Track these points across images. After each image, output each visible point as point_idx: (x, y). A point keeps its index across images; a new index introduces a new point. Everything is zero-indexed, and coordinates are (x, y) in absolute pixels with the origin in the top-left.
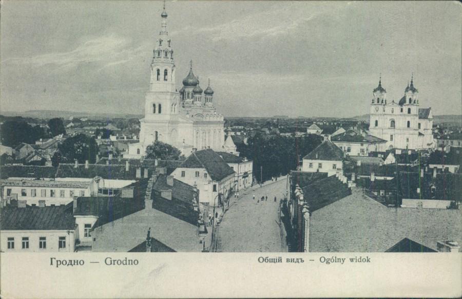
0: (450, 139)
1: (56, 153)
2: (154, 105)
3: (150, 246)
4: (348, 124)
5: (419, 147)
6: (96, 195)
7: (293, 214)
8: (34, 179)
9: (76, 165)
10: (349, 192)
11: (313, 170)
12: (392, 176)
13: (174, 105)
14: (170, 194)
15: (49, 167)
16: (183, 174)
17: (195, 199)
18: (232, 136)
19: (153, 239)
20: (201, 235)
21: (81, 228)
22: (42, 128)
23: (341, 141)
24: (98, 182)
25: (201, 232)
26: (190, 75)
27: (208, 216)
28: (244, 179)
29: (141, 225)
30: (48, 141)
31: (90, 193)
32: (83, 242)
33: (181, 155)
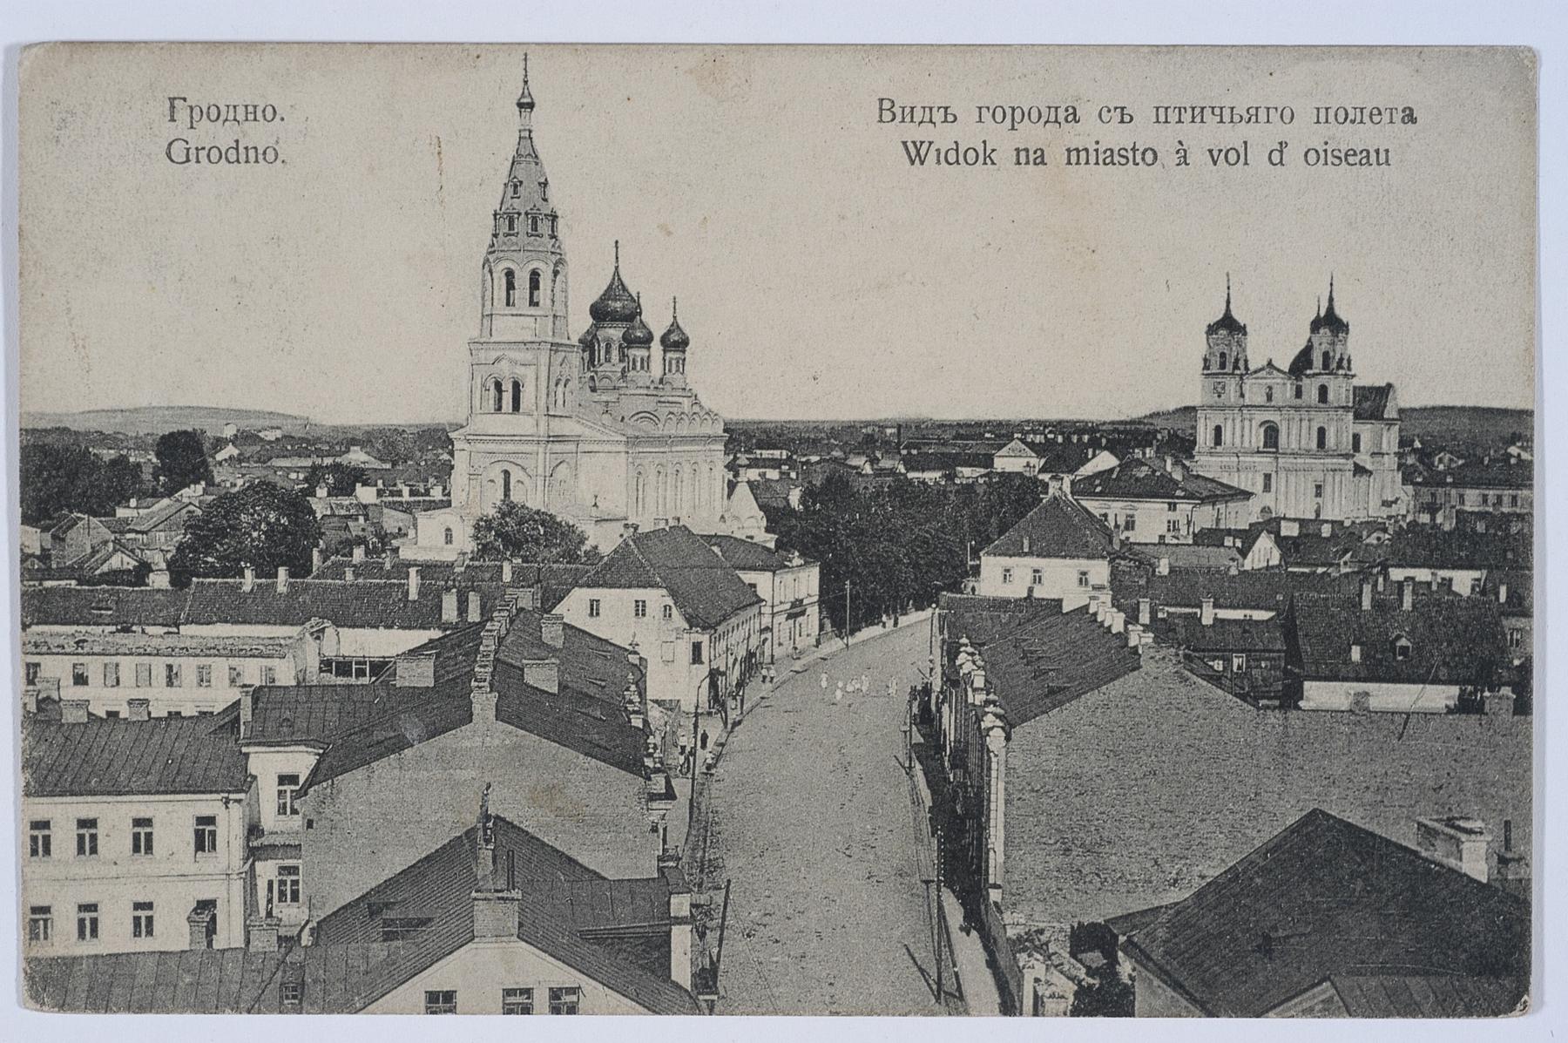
0: (1454, 485)
1: (181, 544)
2: (498, 386)
3: (487, 841)
4: (1125, 437)
6: (314, 678)
8: (113, 628)
9: (249, 580)
10: (1129, 659)
11: (1016, 590)
12: (1268, 609)
14: (554, 672)
16: (594, 609)
17: (633, 688)
20: (655, 805)
22: (138, 465)
23: (1100, 494)
24: (318, 638)
25: (653, 797)
26: (616, 288)
33: (587, 547)
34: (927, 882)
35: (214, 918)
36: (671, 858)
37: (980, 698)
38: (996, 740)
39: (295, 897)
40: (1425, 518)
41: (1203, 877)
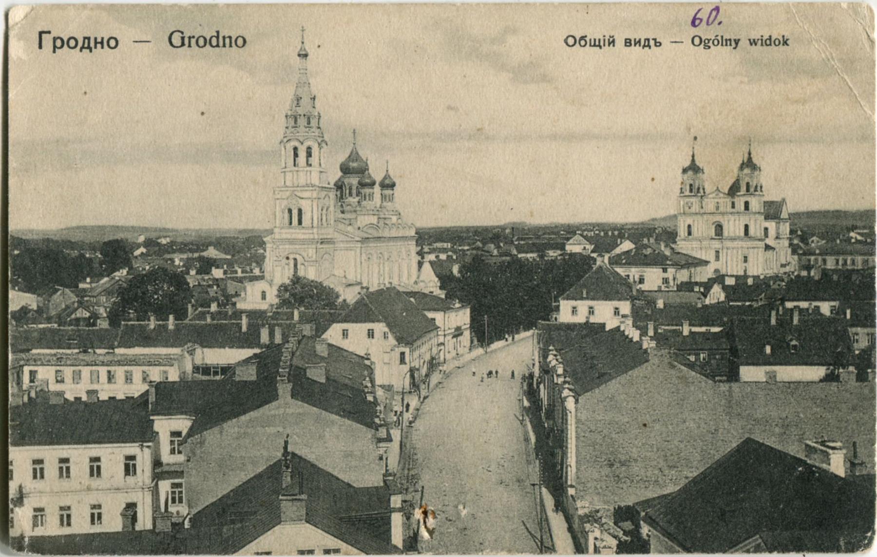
0: (820, 254)
1: (115, 302)
2: (290, 211)
3: (288, 467)
4: (640, 233)
5: (767, 272)
7: (545, 402)
8: (77, 351)
9: (152, 324)
11: (580, 318)
13: (324, 211)
15: (101, 329)
16: (345, 334)
17: (368, 379)
18: (431, 262)
19: (294, 454)
20: (381, 445)
21: (164, 440)
22: (90, 259)
23: (624, 264)
25: (380, 440)
26: (354, 156)
27: (392, 411)
28: (455, 339)
29: (271, 430)
30: (102, 282)
31: (178, 374)
32: (168, 464)
33: (341, 300)
34: (534, 485)
35: (136, 513)
36: (390, 475)
37: (561, 380)
38: (570, 404)
39: (181, 501)
40: (804, 273)
41: (687, 478)
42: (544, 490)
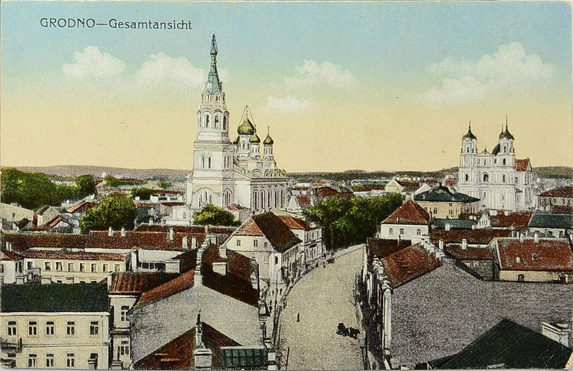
34: (362, 348)
42: (369, 353)
